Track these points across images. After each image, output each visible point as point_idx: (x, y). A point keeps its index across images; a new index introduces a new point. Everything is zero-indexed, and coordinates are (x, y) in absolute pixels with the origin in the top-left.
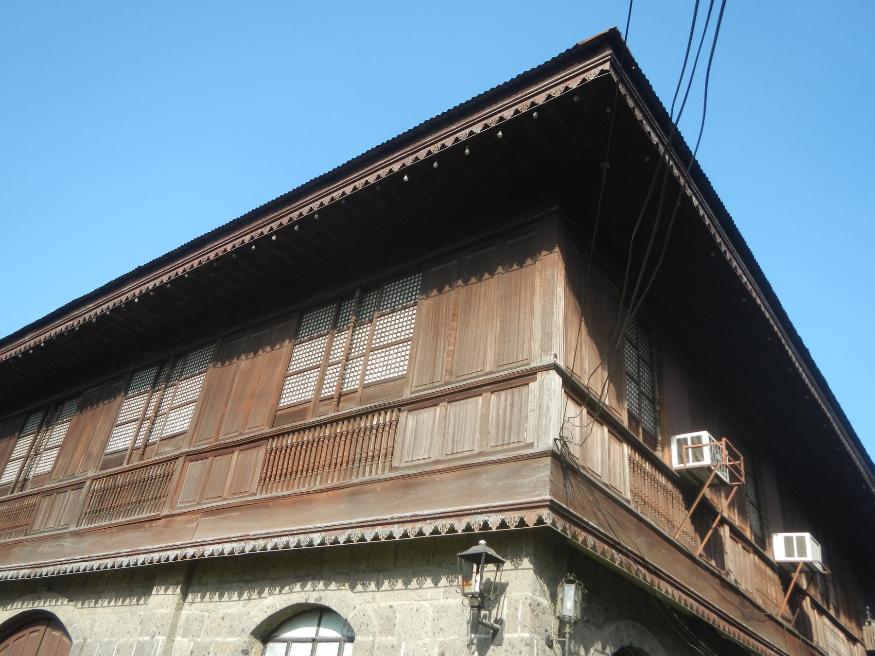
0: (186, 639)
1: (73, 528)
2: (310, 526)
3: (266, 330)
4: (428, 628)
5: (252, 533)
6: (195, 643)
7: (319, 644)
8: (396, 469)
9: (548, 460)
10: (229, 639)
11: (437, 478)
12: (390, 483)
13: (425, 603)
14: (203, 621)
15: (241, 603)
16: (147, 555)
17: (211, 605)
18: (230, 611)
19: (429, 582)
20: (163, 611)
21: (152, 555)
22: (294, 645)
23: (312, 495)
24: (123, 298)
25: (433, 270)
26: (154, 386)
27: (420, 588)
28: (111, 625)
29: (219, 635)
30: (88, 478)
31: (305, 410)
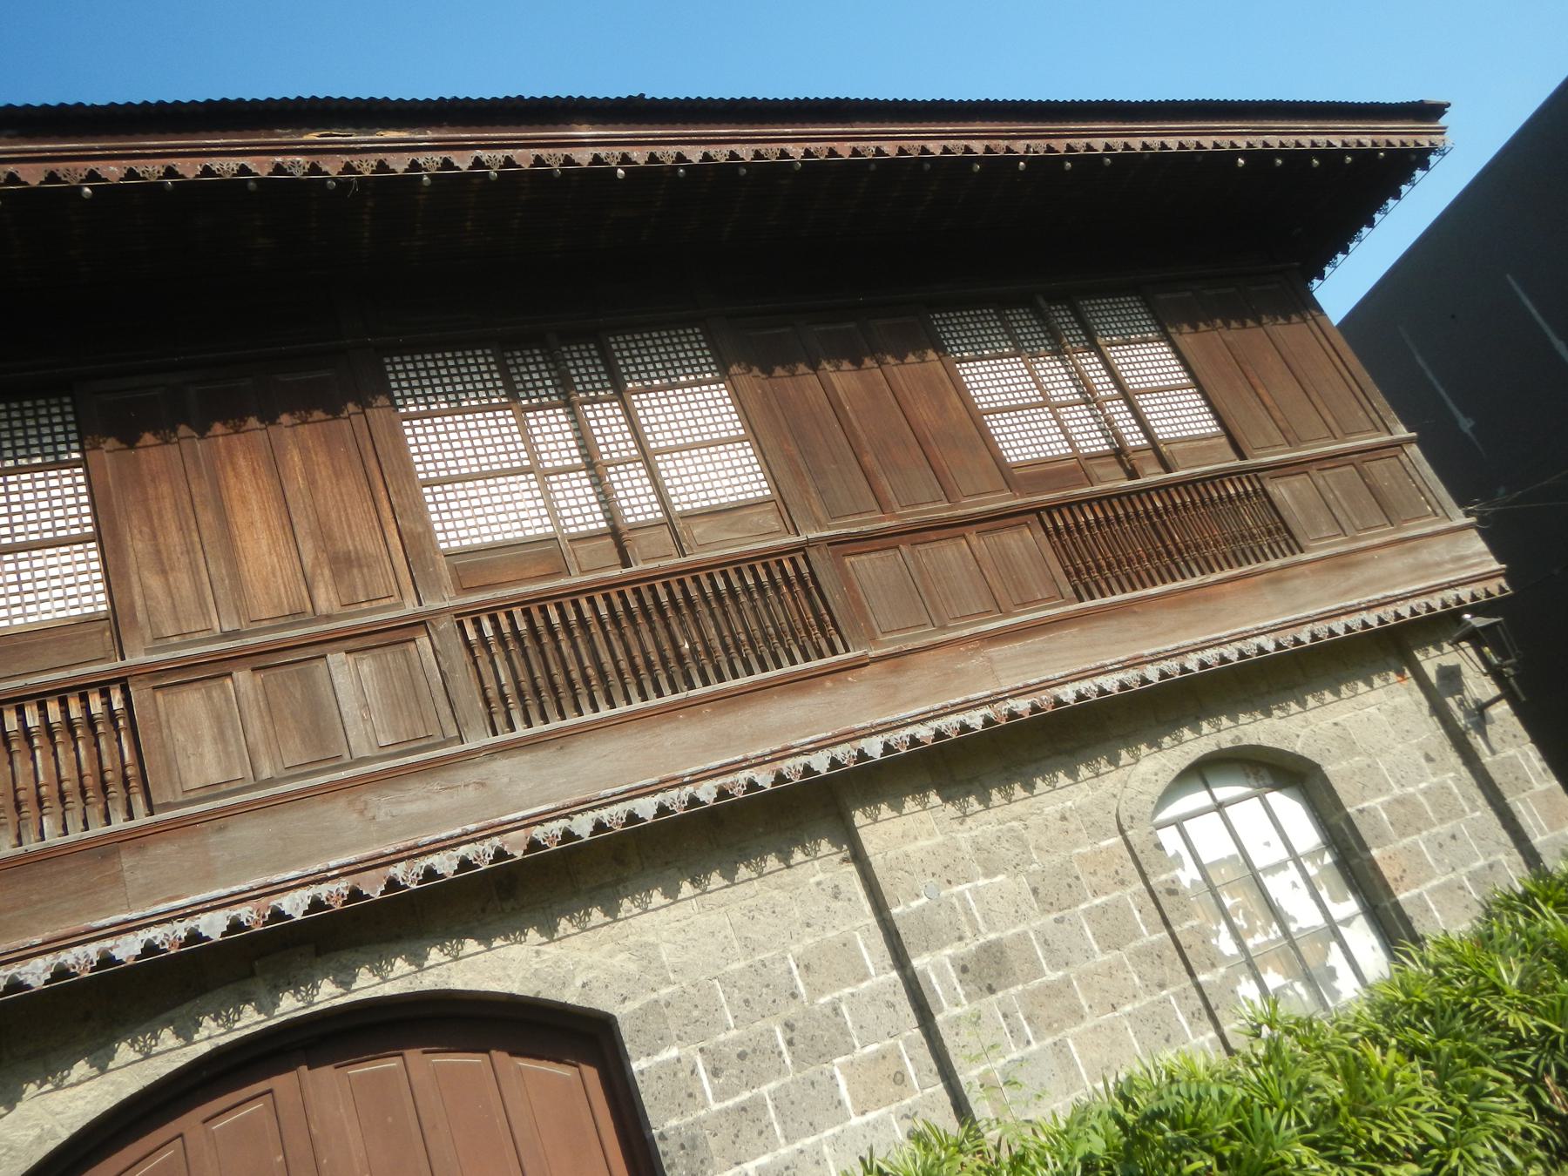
0: (1000, 878)
1: (479, 739)
2: (1248, 628)
3: (852, 325)
4: (1392, 734)
5: (1146, 652)
6: (1028, 875)
7: (1227, 810)
8: (1311, 550)
9: (1474, 533)
10: (1104, 844)
11: (1376, 554)
12: (1319, 565)
13: (1372, 710)
14: (1019, 838)
15: (1084, 785)
16: (886, 736)
17: (1017, 808)
18: (1069, 804)
19: (1362, 687)
20: (923, 843)
21: (909, 731)
22: (1185, 824)
23: (1207, 590)
24: (583, 156)
25: (1161, 297)
26: (513, 394)
27: (1356, 694)
28: (729, 930)
29: (1076, 844)
30: (442, 611)
31: (1072, 470)
